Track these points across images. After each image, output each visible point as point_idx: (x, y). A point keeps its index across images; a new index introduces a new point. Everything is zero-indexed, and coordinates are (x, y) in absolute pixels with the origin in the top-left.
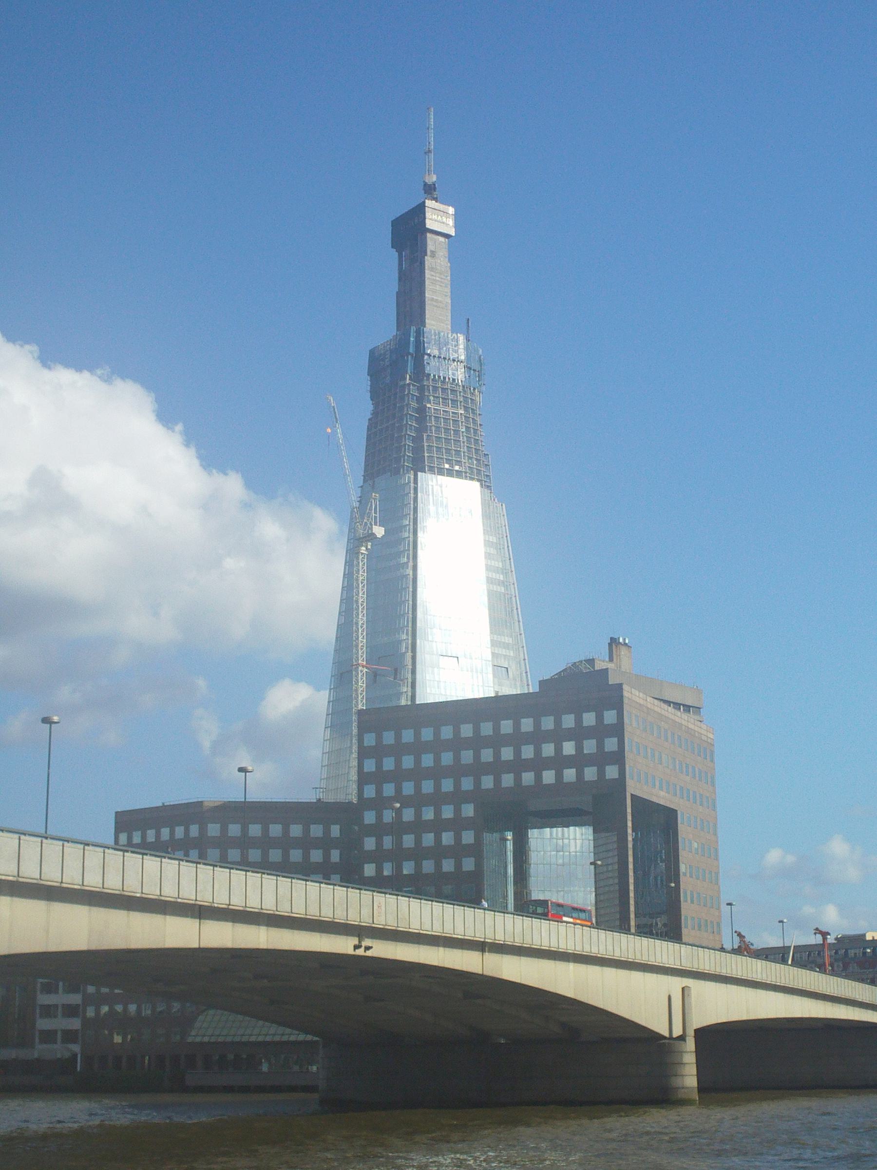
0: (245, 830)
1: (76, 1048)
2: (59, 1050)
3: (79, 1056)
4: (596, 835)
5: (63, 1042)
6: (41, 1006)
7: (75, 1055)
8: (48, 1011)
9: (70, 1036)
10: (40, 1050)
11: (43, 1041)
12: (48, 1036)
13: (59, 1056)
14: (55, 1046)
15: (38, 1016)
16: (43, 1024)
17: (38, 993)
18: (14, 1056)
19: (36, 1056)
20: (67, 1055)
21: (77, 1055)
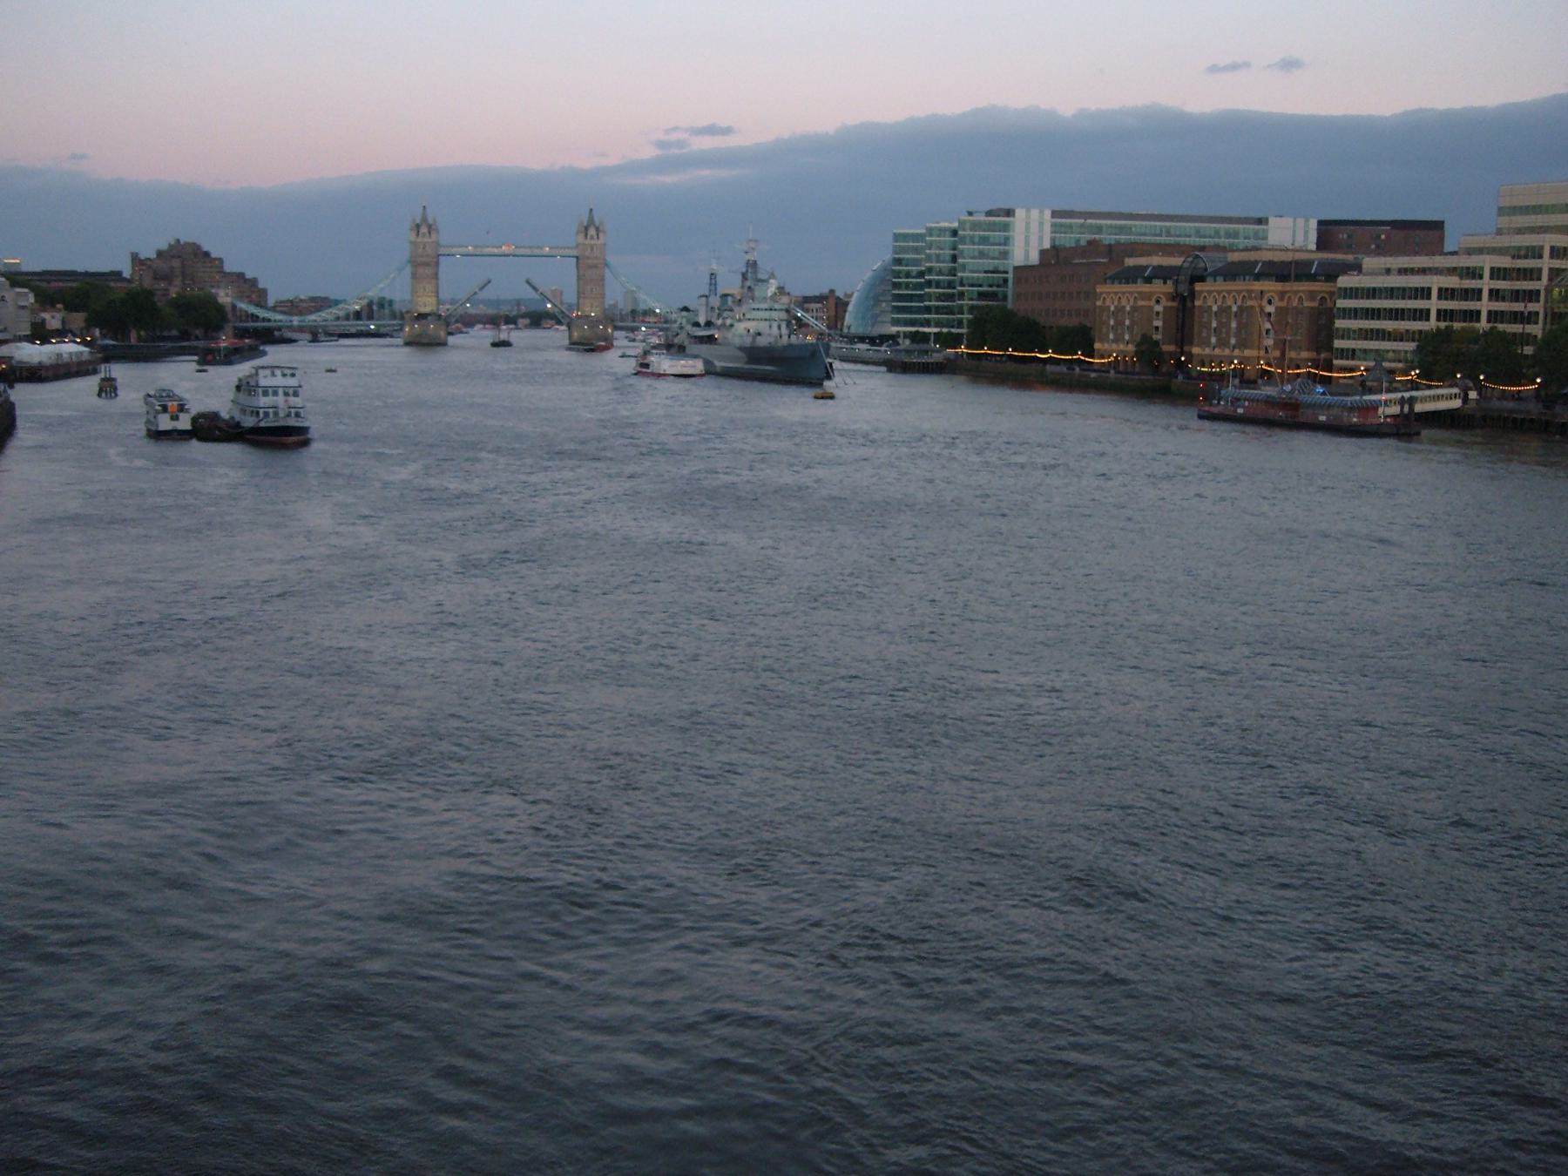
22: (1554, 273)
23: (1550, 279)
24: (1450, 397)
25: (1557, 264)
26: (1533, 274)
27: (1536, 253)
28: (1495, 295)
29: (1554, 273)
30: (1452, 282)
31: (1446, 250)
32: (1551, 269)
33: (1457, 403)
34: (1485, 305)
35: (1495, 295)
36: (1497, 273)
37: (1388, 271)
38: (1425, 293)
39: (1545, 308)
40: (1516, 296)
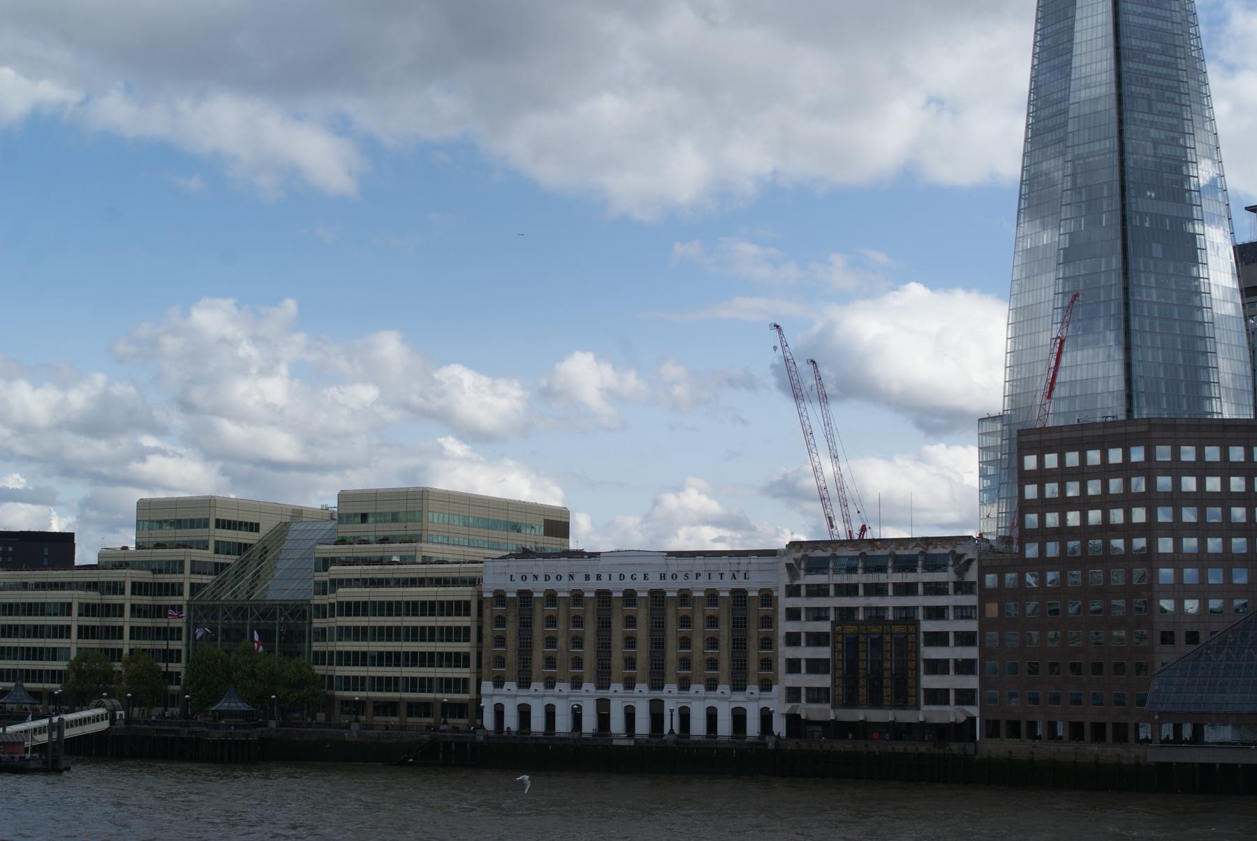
0: (1200, 454)
1: (974, 711)
2: (951, 713)
3: (978, 720)
4: (566, 520)
5: (958, 702)
6: (925, 660)
7: (972, 720)
8: (938, 667)
9: (965, 697)
10: (929, 713)
11: (927, 703)
12: (938, 697)
13: (952, 720)
14: (946, 708)
15: (922, 673)
16: (929, 682)
17: (922, 645)
18: (891, 719)
19: (921, 719)
20: (962, 719)
21: (974, 719)
22: (195, 588)
23: (192, 593)
24: (97, 719)
25: (198, 579)
26: (175, 589)
27: (177, 566)
28: (137, 611)
29: (195, 588)
30: (93, 597)
31: (77, 562)
32: (192, 585)
33: (104, 725)
34: (127, 621)
35: (137, 611)
36: (138, 588)
37: (25, 586)
38: (66, 609)
39: (188, 622)
40: (159, 611)
